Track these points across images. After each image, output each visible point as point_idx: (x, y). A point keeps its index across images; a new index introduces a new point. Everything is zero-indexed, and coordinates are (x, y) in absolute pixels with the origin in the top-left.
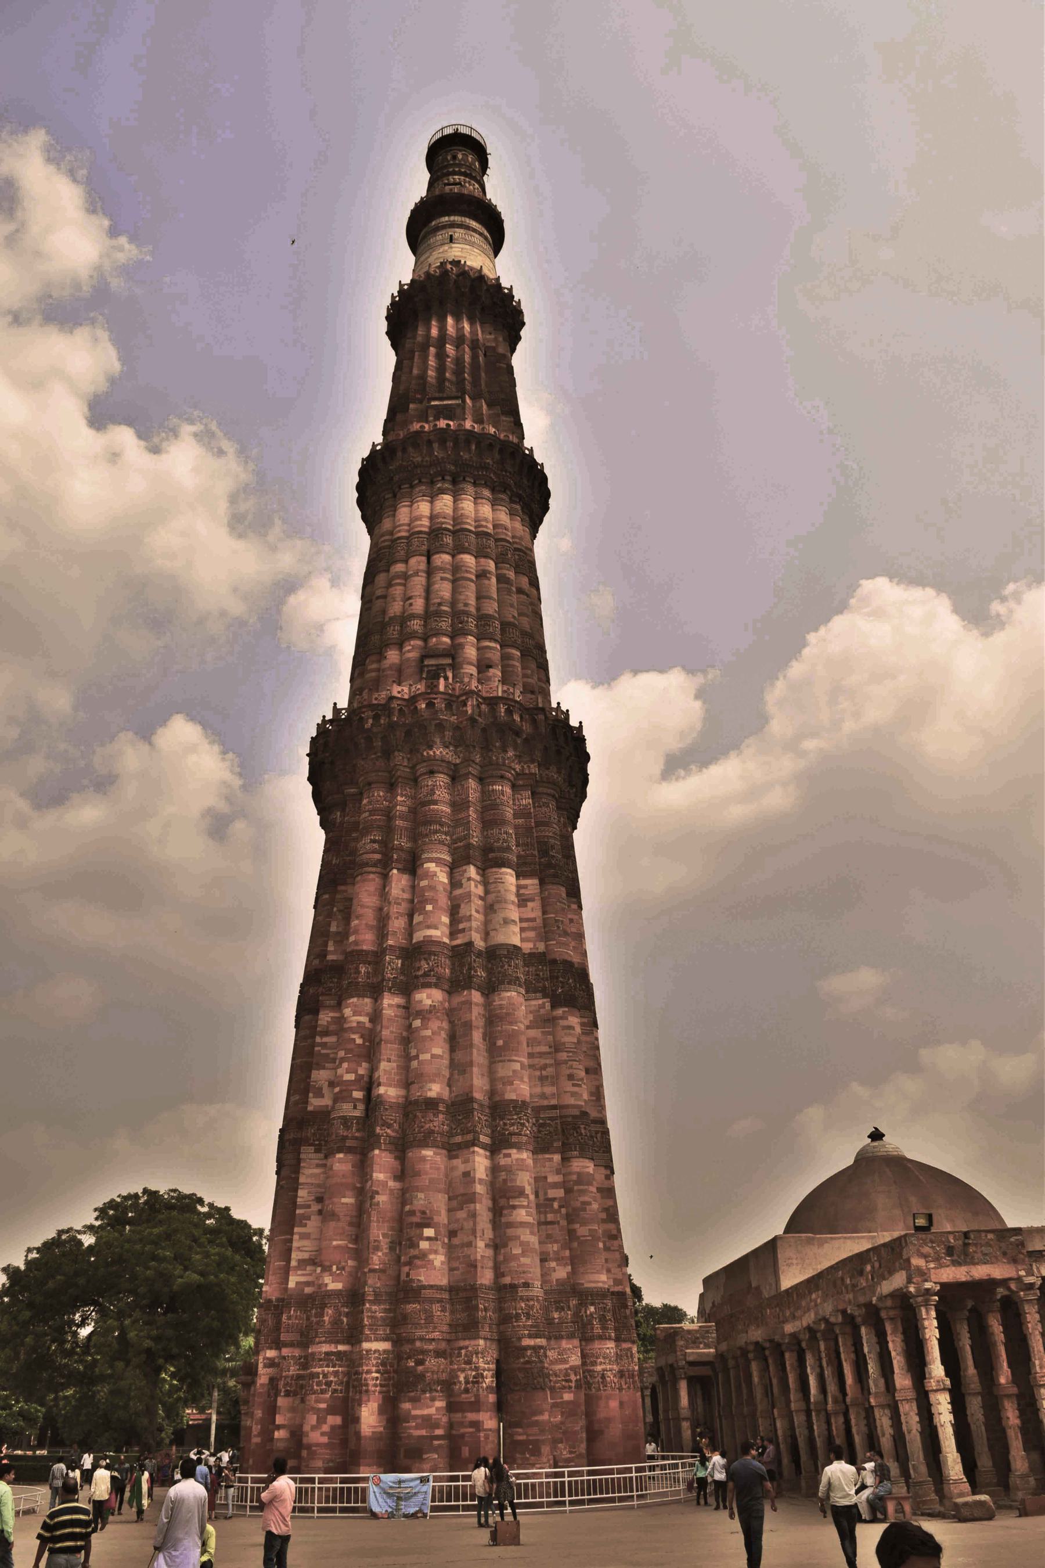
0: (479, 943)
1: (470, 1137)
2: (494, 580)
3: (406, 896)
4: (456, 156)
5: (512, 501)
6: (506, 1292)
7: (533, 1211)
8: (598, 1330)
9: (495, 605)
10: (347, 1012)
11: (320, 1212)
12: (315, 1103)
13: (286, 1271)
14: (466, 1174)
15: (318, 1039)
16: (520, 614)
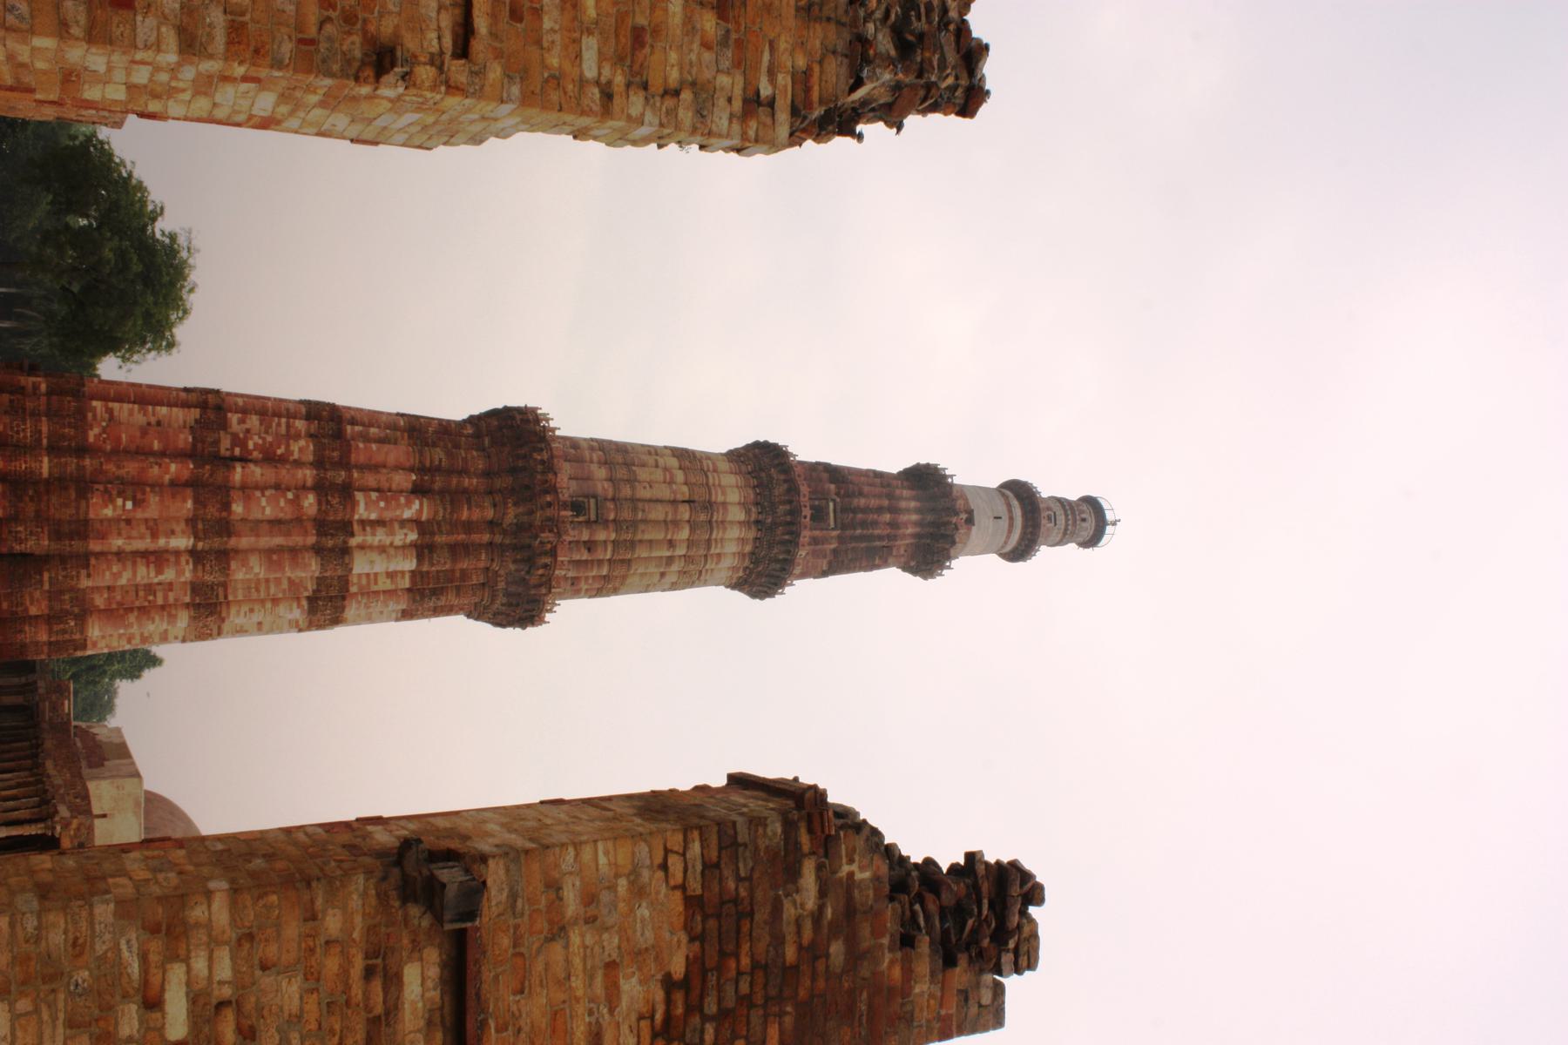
0: (353, 542)
1: (201, 535)
2: (668, 554)
3: (394, 487)
4: (1086, 521)
5: (745, 569)
6: (84, 561)
7: (146, 581)
8: (56, 628)
9: (644, 555)
10: (302, 443)
11: (149, 424)
12: (234, 418)
13: (105, 398)
14: (173, 532)
15: (284, 420)
16: (643, 575)
